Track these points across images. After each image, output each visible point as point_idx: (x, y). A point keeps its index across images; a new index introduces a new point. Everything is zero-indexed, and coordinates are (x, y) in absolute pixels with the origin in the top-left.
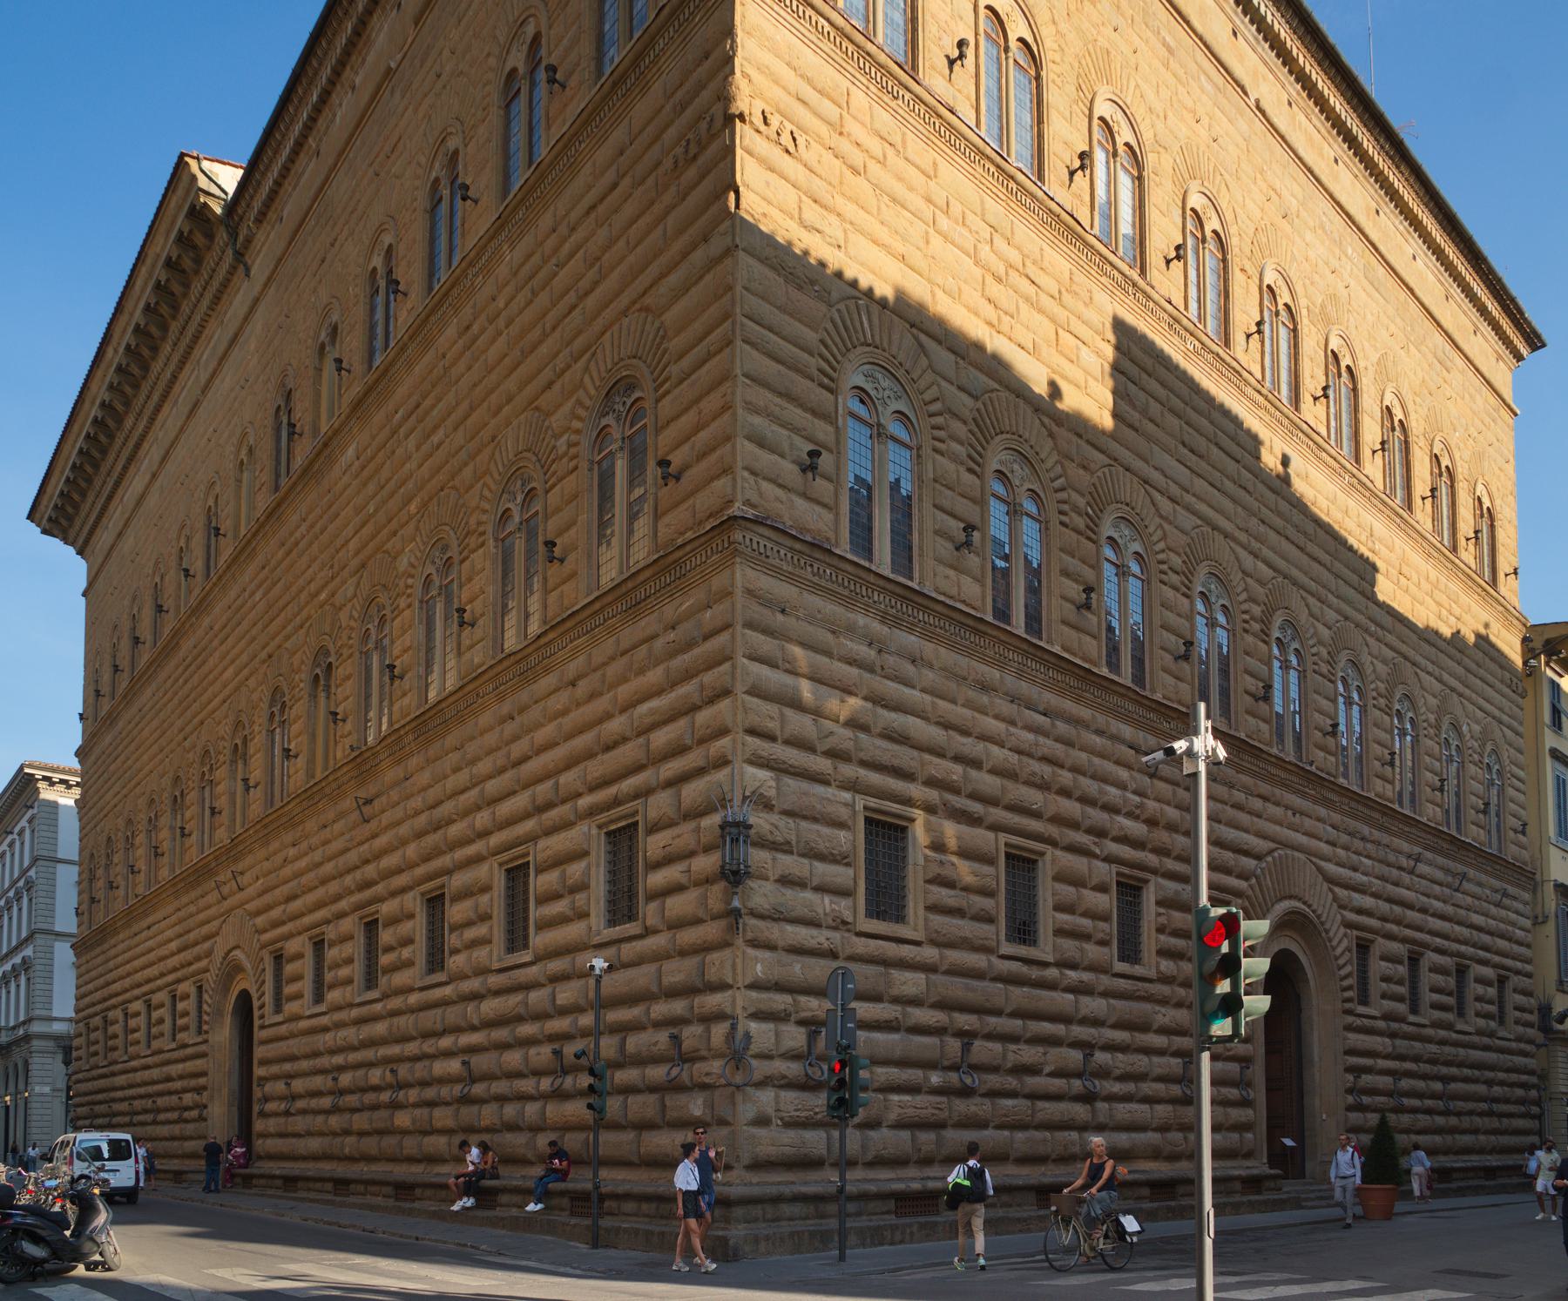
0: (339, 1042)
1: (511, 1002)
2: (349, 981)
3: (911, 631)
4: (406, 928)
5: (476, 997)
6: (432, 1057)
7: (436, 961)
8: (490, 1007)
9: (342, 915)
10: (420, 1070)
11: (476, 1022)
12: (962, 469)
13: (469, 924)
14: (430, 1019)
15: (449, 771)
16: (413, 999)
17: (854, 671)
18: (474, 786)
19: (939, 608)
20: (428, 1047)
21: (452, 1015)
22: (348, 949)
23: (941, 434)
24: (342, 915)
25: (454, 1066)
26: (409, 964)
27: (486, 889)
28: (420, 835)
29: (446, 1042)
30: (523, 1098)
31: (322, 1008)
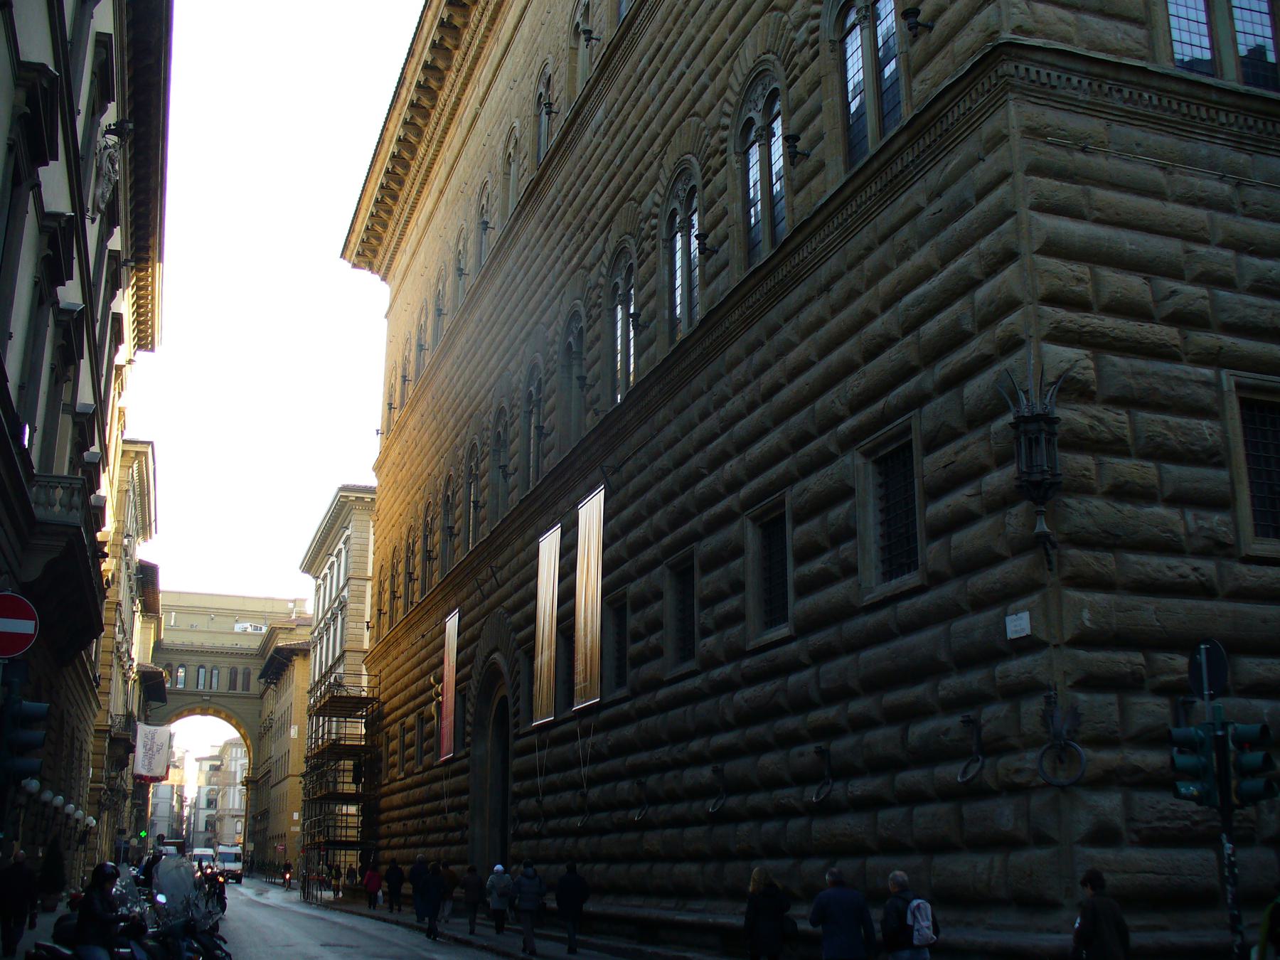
5: (728, 686)
6: (680, 765)
11: (730, 717)
25: (705, 773)
30: (785, 813)
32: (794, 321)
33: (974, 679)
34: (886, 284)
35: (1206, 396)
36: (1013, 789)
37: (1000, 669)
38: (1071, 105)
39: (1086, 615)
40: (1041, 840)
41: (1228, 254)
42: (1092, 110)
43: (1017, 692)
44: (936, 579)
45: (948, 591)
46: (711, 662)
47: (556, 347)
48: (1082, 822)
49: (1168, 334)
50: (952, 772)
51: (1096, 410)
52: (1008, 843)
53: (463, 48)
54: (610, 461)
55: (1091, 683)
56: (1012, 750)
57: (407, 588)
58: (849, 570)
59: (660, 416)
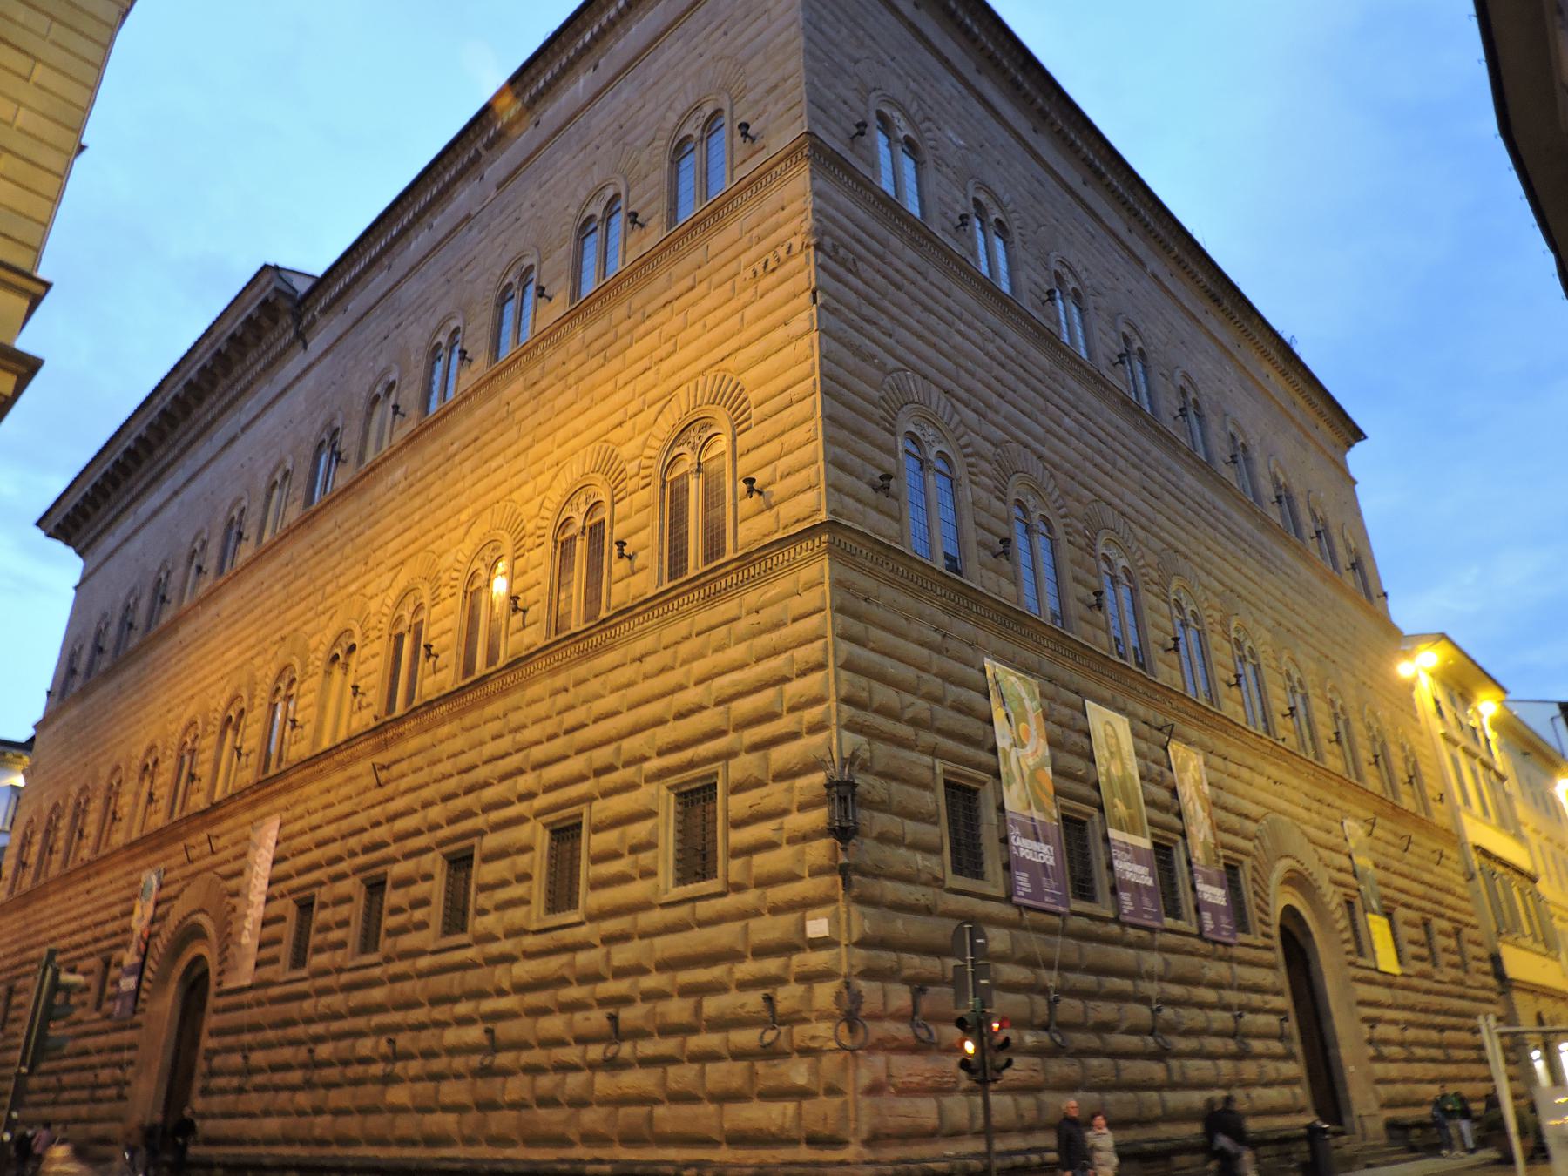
0: (320, 1009)
1: (552, 965)
2: (341, 945)
3: (966, 620)
4: (419, 890)
5: (508, 959)
7: (456, 918)
8: (524, 970)
9: (341, 877)
10: (427, 1039)
12: (992, 497)
13: (504, 883)
14: (441, 984)
15: (488, 738)
16: (424, 963)
17: (925, 652)
18: (518, 751)
19: (989, 602)
20: (440, 1013)
21: (472, 978)
22: (343, 911)
23: (974, 470)
24: (341, 877)
25: (474, 1034)
26: (422, 925)
27: (526, 849)
28: (446, 798)
29: (463, 1008)
30: (565, 1068)
31: (303, 973)
32: (602, 678)
33: (772, 966)
34: (699, 667)
35: (926, 775)
36: (805, 1052)
37: (796, 959)
38: (860, 568)
39: (867, 923)
40: (832, 1091)
41: (939, 680)
42: (871, 573)
43: (808, 978)
44: (738, 888)
45: (750, 898)
46: (490, 938)
47: (320, 655)
48: (865, 1078)
49: (905, 731)
50: (746, 1038)
51: (870, 779)
52: (801, 1094)
53: (232, 378)
54: (382, 758)
55: (869, 974)
56: (806, 1021)
57: (69, 843)
58: (648, 873)
59: (445, 730)
